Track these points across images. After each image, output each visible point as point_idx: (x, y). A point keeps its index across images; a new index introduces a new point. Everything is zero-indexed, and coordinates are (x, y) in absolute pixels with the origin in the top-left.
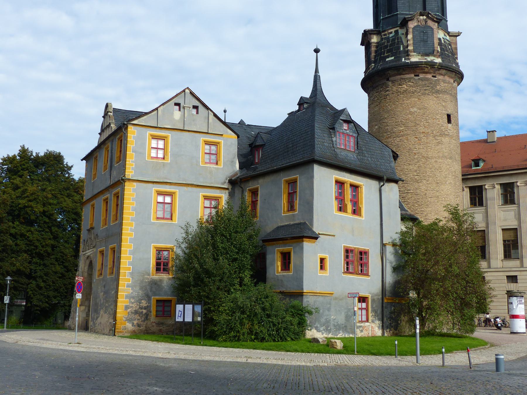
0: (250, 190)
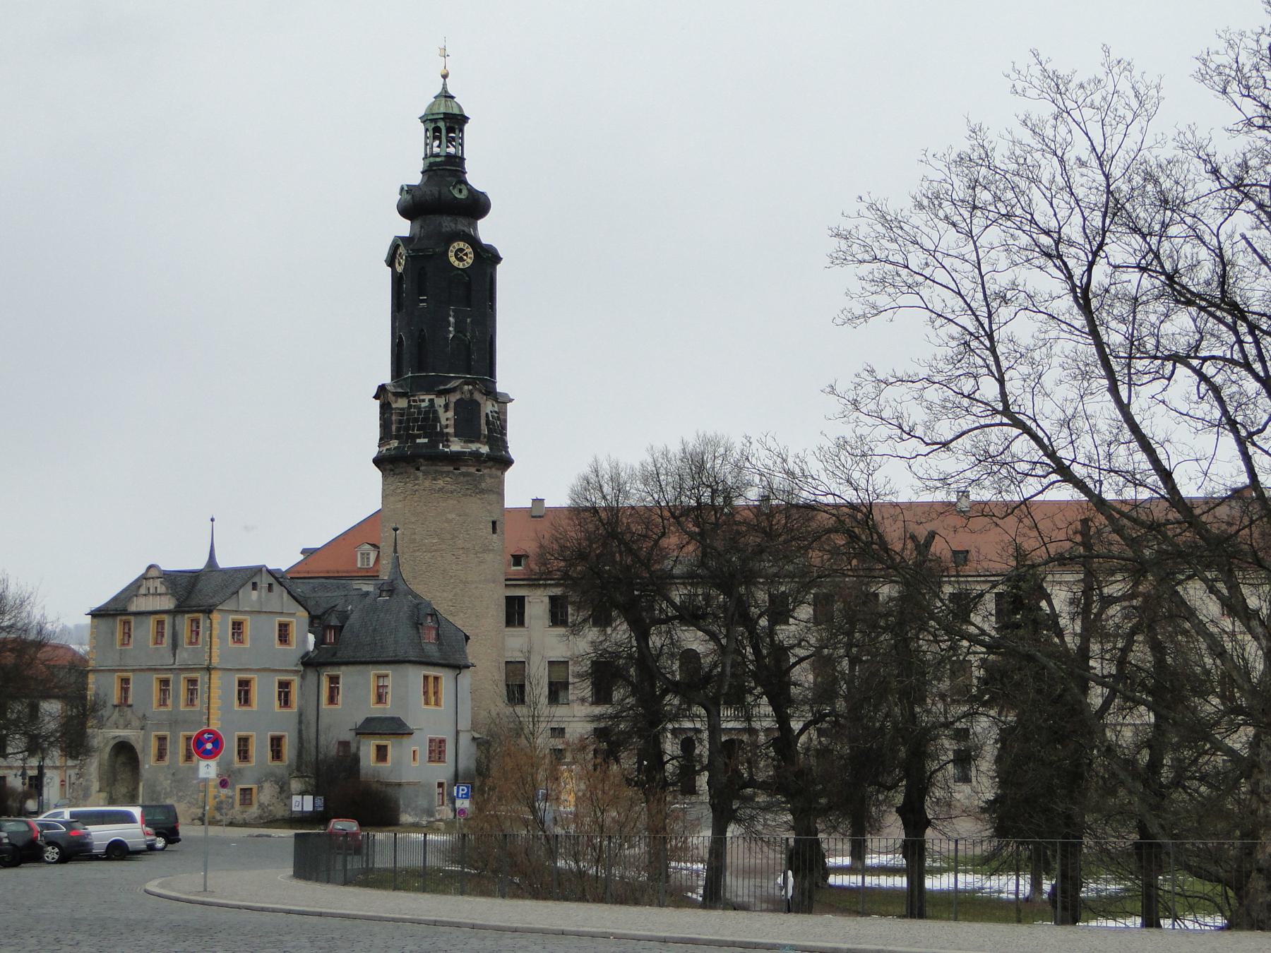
0: (328, 675)
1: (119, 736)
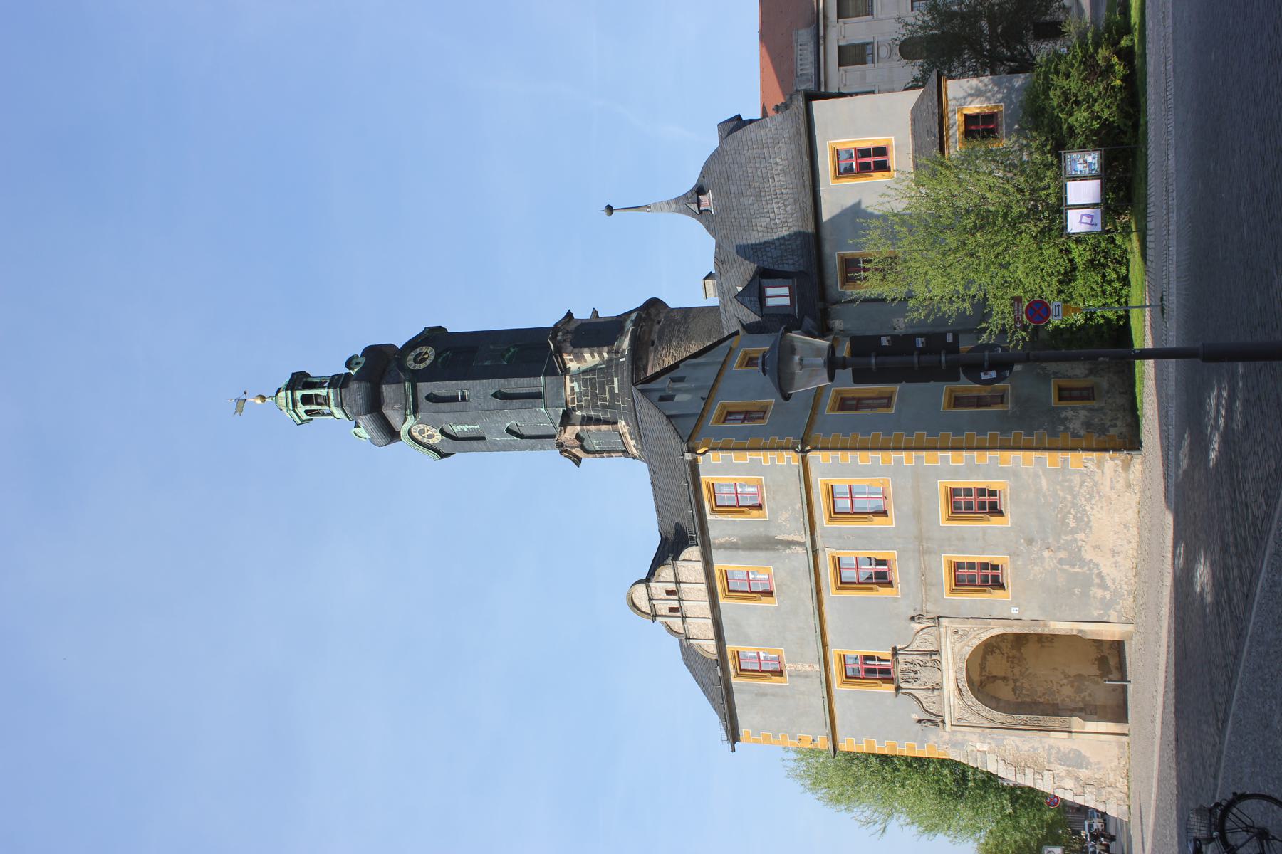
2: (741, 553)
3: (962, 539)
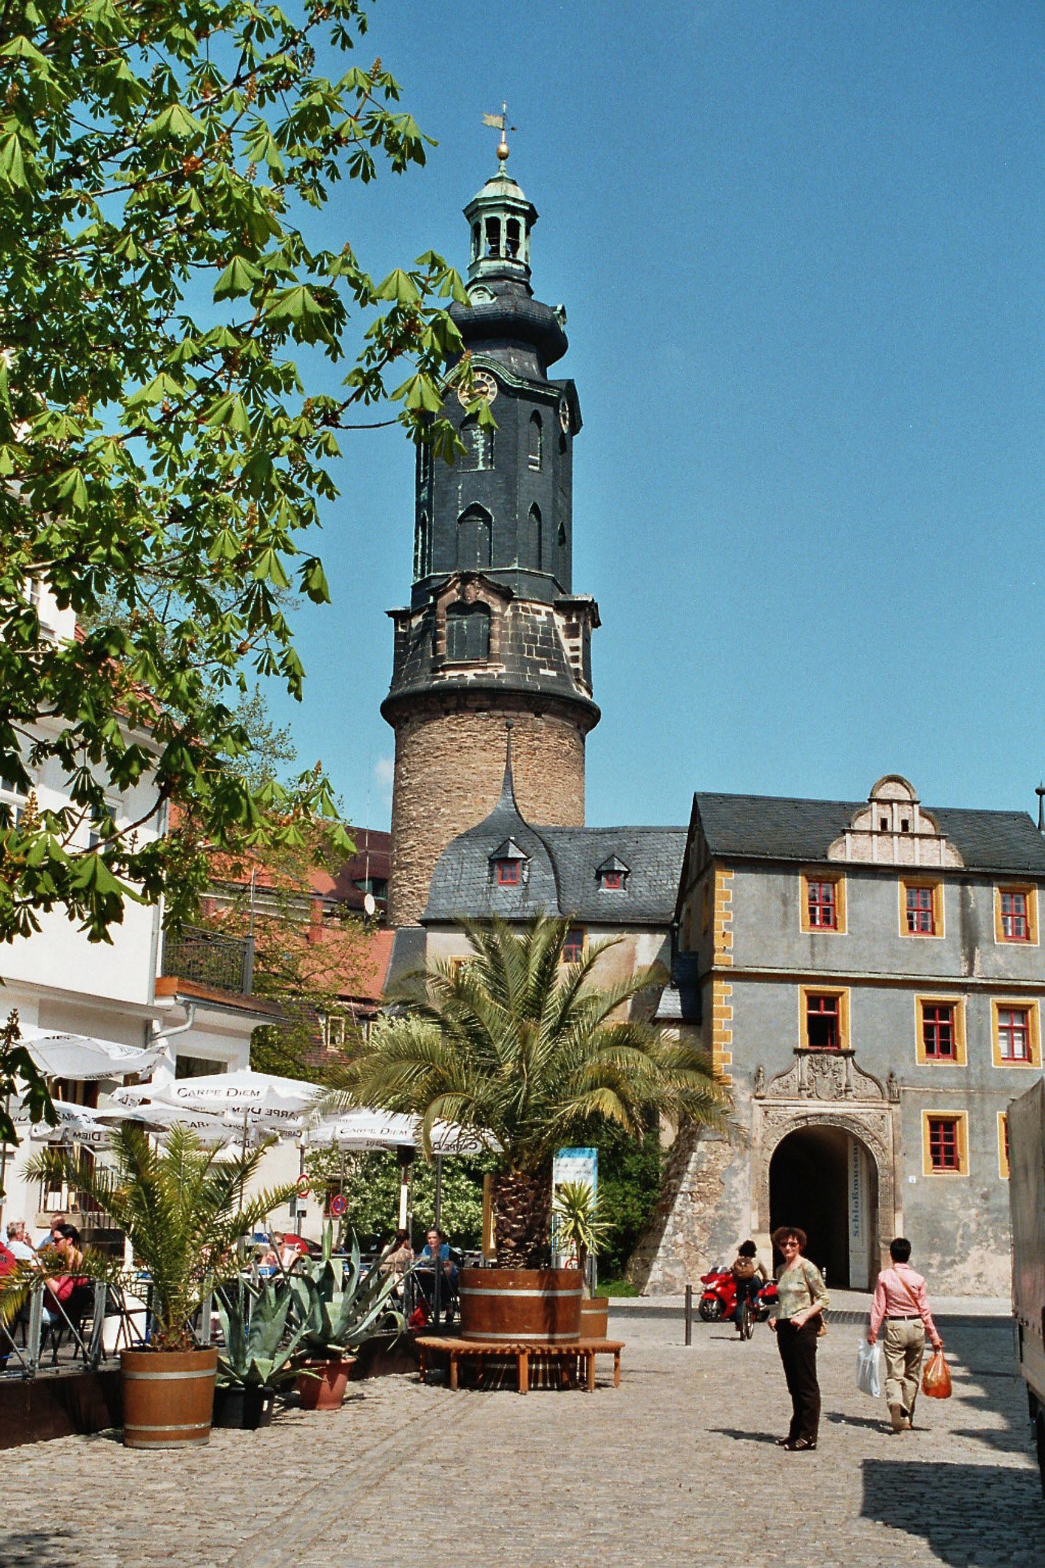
1: (821, 1115)
2: (958, 910)
3: (984, 1132)
